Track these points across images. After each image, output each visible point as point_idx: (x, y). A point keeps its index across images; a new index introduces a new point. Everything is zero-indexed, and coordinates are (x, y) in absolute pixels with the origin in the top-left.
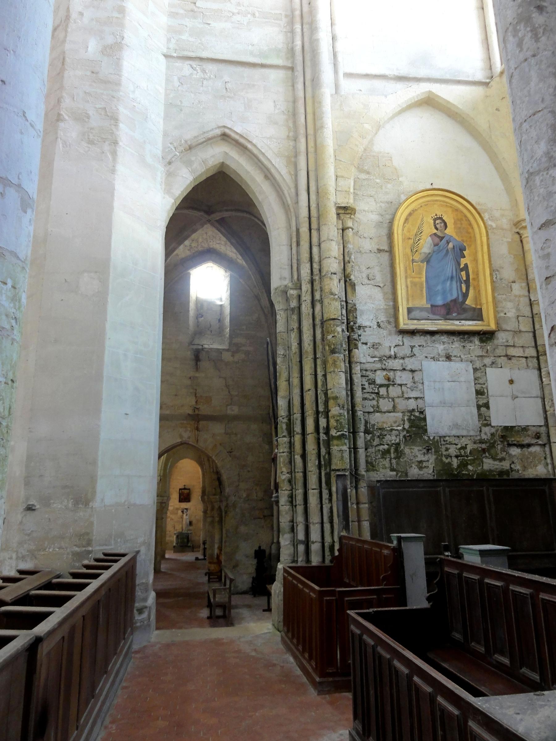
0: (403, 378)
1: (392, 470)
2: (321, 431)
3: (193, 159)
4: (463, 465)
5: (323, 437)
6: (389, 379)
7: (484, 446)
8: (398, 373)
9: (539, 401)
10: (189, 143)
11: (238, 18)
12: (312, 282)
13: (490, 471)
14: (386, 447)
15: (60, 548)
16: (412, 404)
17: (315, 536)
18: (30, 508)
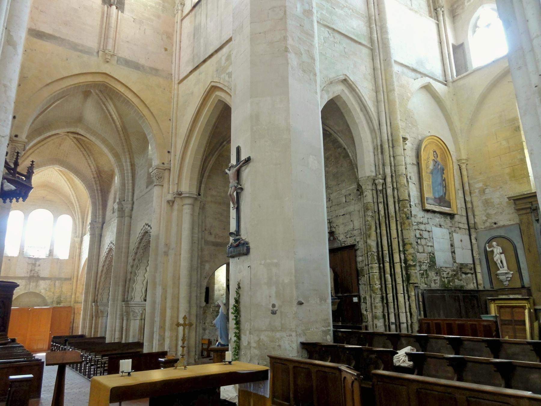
0: (425, 235)
1: (426, 284)
2: (403, 261)
3: (329, 90)
4: (449, 282)
5: (403, 265)
6: (421, 235)
7: (454, 273)
8: (424, 232)
9: (470, 251)
10: (331, 80)
11: (346, 10)
12: (392, 176)
13: (458, 286)
14: (422, 271)
15: (316, 328)
16: (430, 249)
17: (403, 319)
18: (300, 303)
